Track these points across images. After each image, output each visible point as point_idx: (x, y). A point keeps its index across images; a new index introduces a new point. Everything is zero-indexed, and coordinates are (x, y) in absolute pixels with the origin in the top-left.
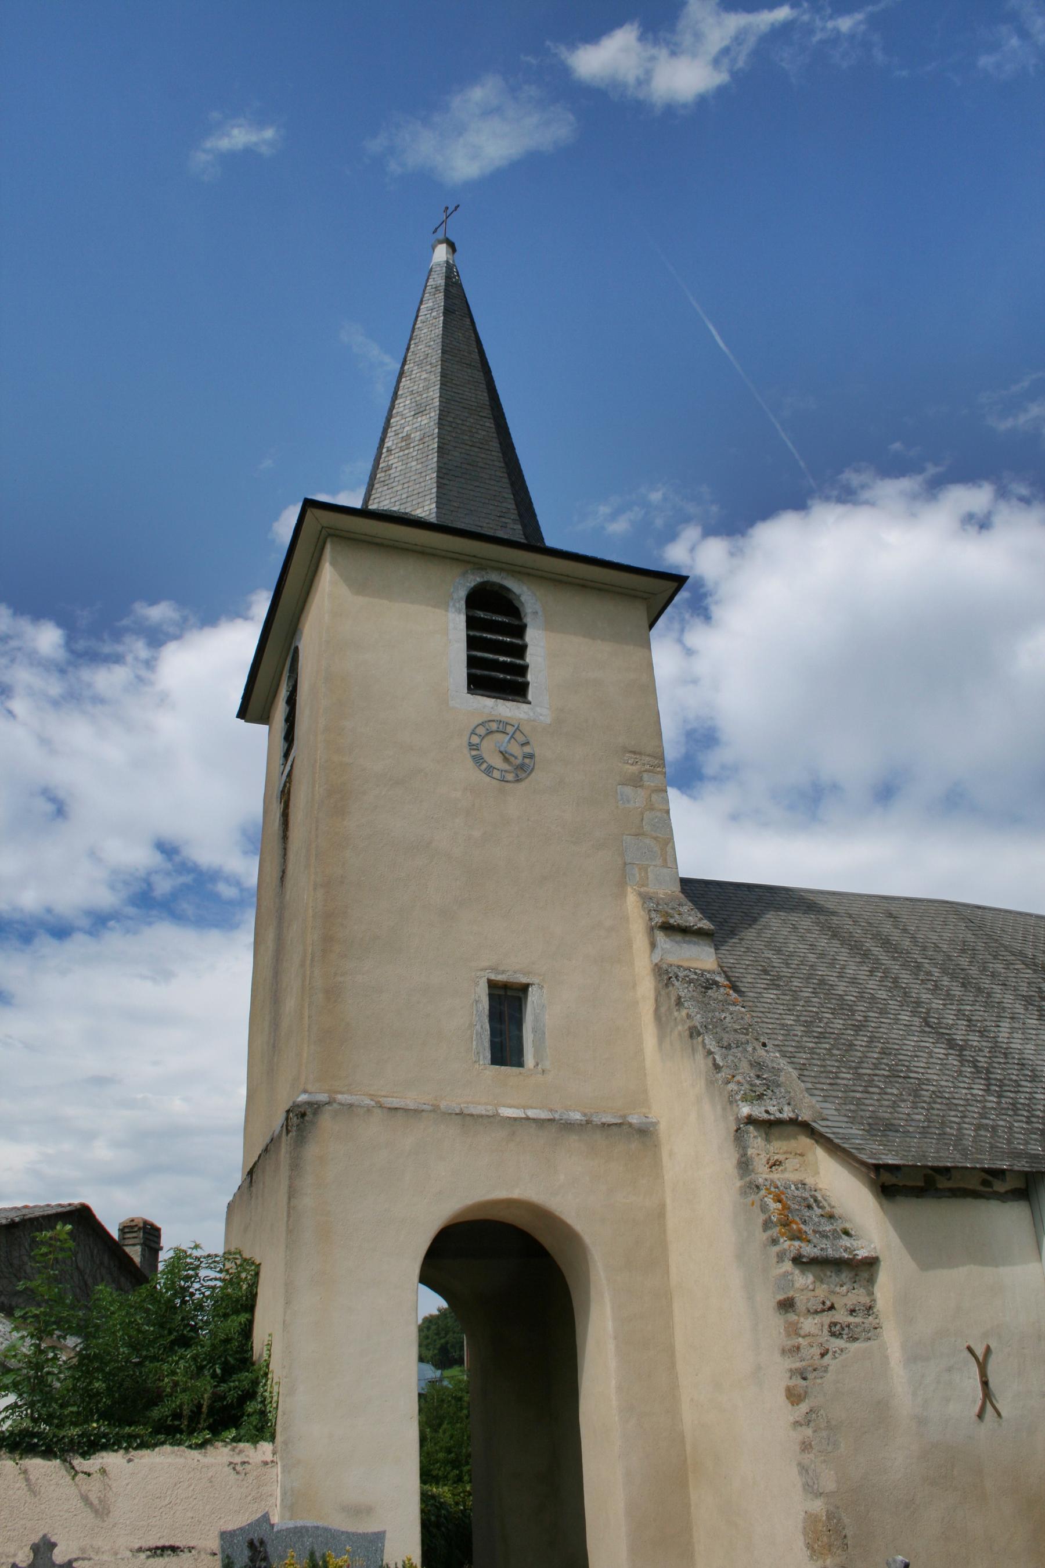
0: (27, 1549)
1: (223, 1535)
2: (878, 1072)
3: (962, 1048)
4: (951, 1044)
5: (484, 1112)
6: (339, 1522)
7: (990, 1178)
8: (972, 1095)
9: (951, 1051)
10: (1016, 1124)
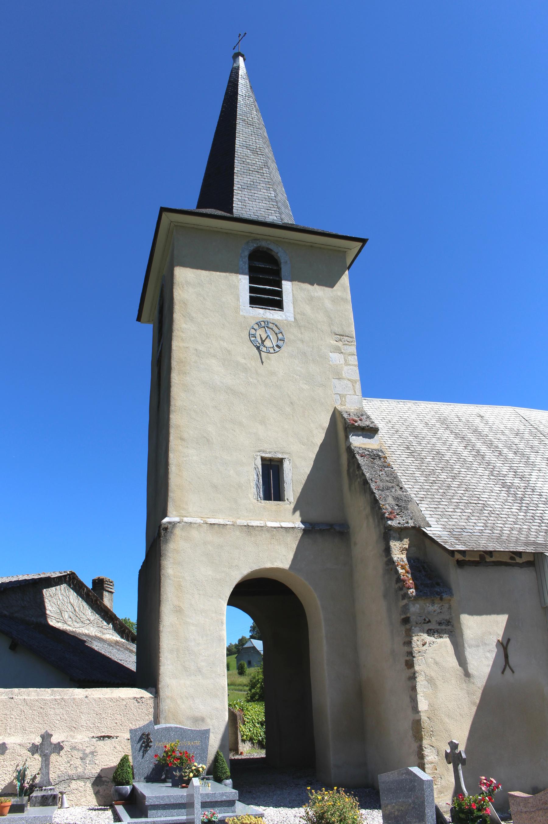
0: (39, 737)
1: (131, 731)
2: (462, 501)
3: (509, 487)
4: (504, 485)
5: (259, 525)
6: (188, 726)
7: (514, 556)
8: (511, 512)
9: (503, 489)
10: (533, 527)
